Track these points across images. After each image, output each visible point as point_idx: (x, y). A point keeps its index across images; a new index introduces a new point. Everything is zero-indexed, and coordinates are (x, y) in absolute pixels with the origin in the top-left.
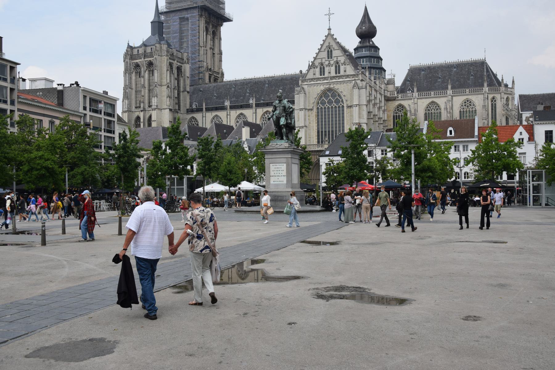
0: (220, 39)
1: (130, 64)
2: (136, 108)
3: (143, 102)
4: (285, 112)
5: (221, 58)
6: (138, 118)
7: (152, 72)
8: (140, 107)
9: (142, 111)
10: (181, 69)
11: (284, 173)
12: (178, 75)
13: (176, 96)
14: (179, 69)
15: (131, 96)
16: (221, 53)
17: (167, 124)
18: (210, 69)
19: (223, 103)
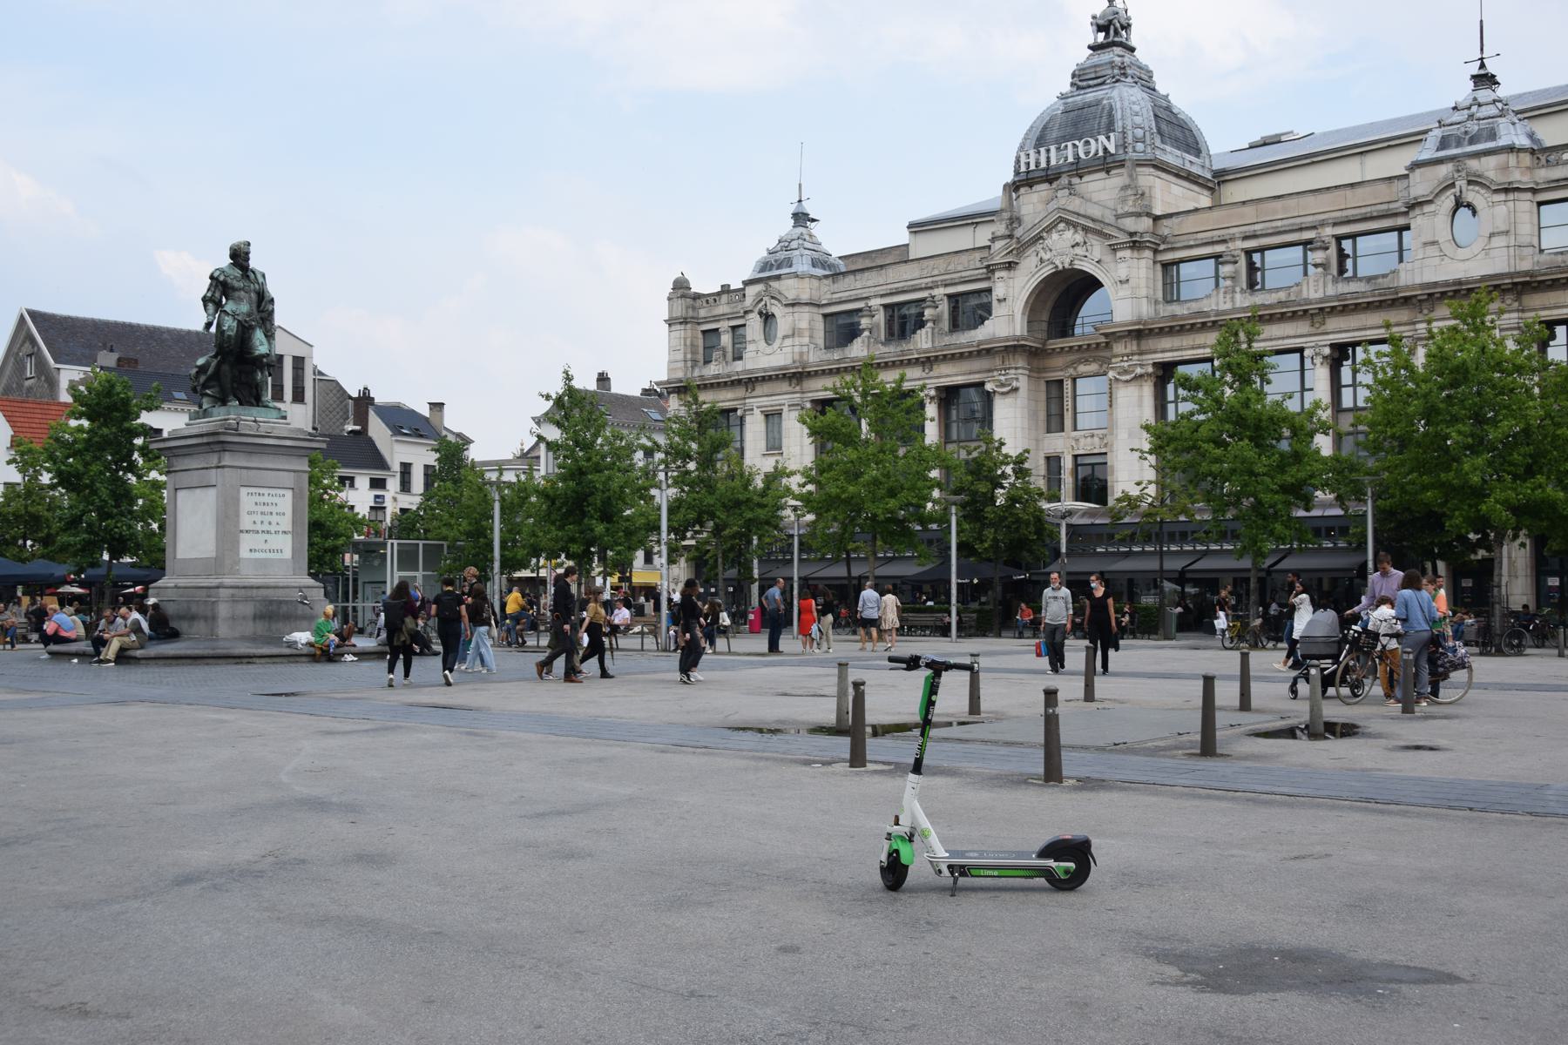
11: (286, 523)
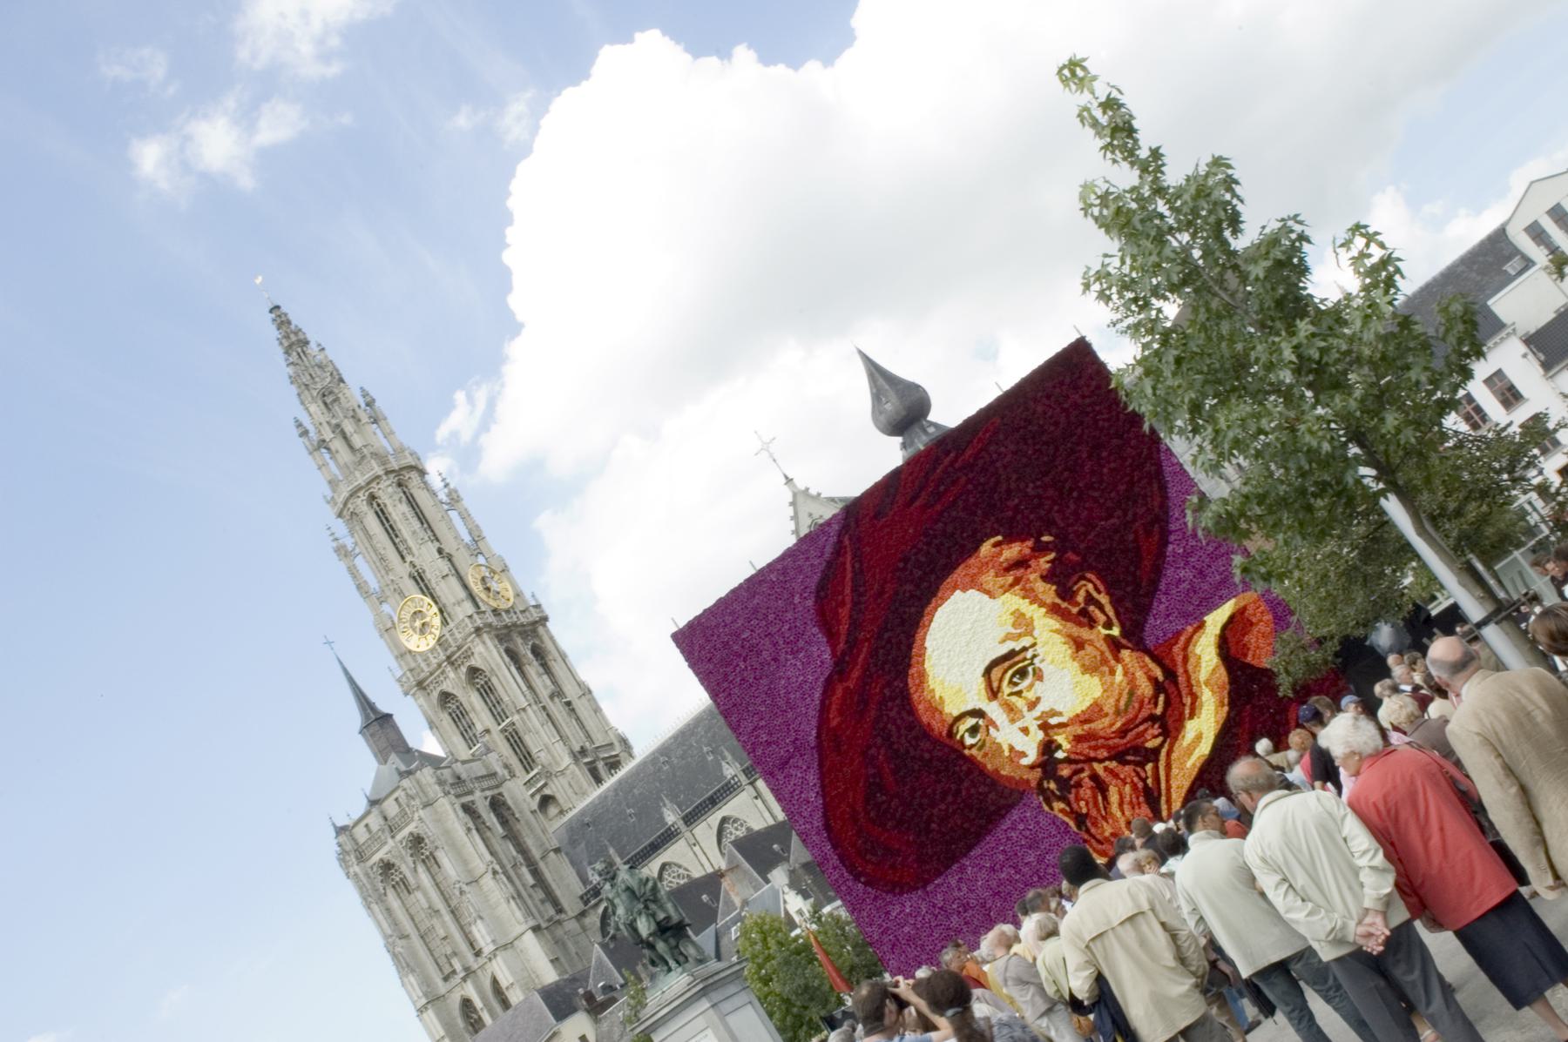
0: (563, 657)
1: (367, 875)
2: (446, 979)
3: (455, 954)
4: (638, 899)
5: (592, 701)
6: (467, 1004)
7: (430, 862)
8: (454, 972)
9: (464, 979)
10: (504, 803)
12: (504, 822)
13: (530, 880)
14: (497, 805)
15: (414, 954)
16: (586, 692)
17: (550, 976)
18: (583, 751)
19: (661, 819)
